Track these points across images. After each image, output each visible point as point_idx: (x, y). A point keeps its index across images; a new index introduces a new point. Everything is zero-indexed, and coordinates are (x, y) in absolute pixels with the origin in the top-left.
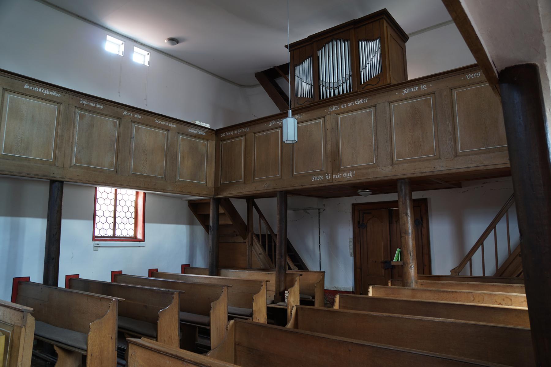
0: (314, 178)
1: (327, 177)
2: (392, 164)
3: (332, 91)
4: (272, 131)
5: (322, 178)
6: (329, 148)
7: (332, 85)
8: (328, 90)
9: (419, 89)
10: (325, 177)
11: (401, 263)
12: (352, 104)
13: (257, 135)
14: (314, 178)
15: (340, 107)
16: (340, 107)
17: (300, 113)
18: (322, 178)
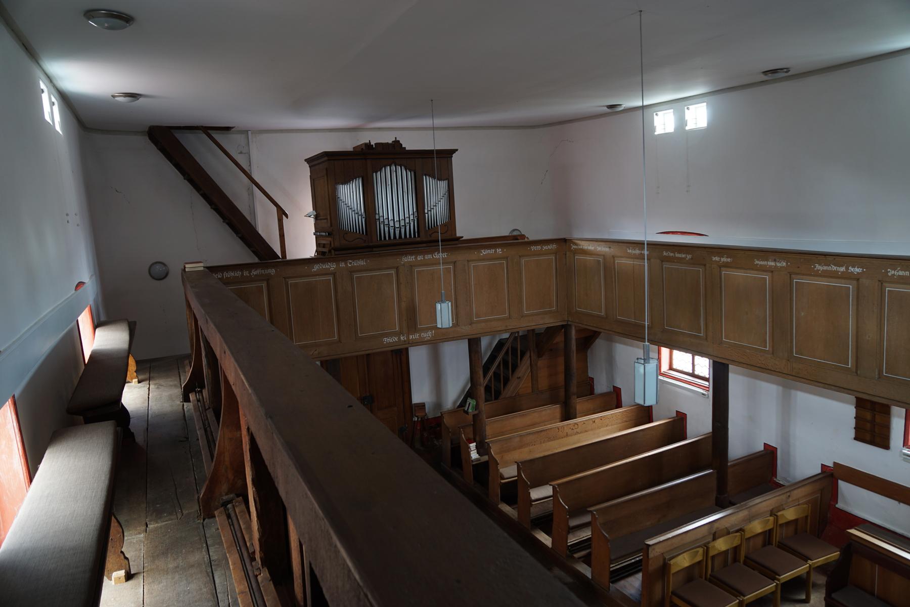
0: (387, 340)
1: (402, 338)
2: (471, 324)
3: (392, 231)
4: (318, 278)
5: (396, 339)
6: (404, 305)
7: (391, 224)
8: (386, 229)
9: (496, 251)
10: (399, 339)
11: (476, 412)
12: (430, 256)
13: (290, 282)
14: (387, 340)
15: (416, 258)
16: (416, 258)
17: (362, 259)
18: (396, 339)
